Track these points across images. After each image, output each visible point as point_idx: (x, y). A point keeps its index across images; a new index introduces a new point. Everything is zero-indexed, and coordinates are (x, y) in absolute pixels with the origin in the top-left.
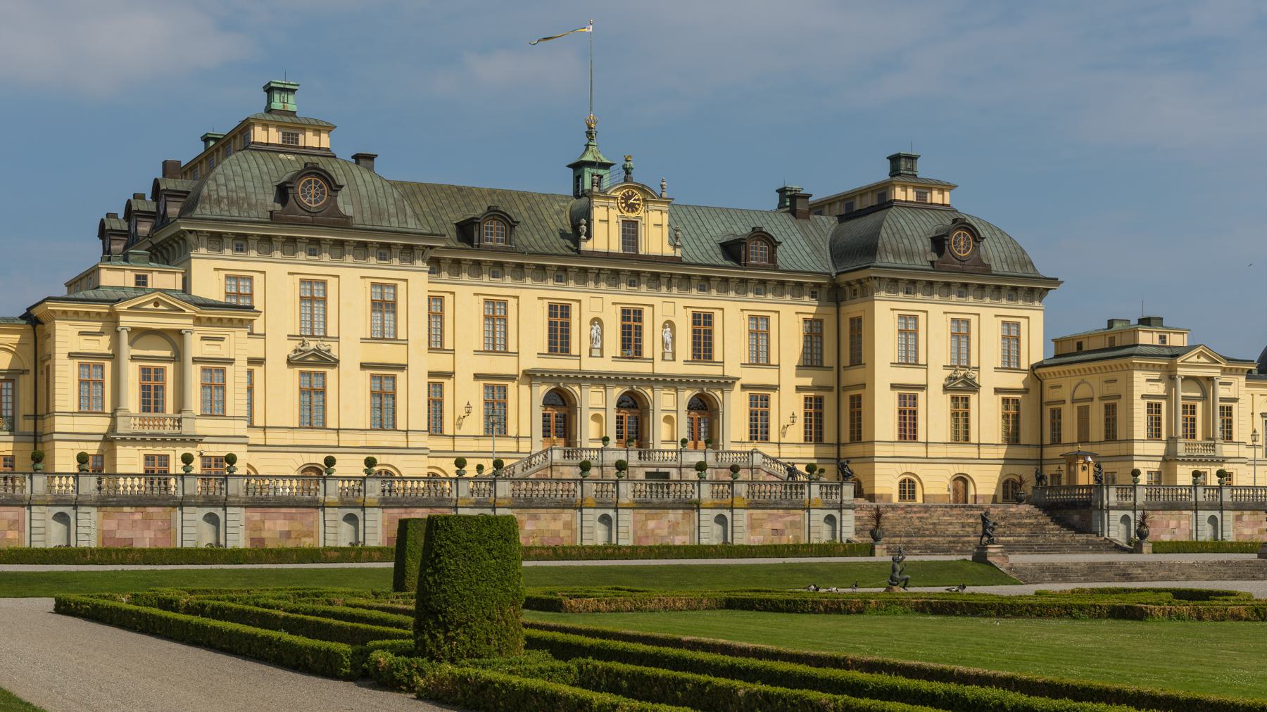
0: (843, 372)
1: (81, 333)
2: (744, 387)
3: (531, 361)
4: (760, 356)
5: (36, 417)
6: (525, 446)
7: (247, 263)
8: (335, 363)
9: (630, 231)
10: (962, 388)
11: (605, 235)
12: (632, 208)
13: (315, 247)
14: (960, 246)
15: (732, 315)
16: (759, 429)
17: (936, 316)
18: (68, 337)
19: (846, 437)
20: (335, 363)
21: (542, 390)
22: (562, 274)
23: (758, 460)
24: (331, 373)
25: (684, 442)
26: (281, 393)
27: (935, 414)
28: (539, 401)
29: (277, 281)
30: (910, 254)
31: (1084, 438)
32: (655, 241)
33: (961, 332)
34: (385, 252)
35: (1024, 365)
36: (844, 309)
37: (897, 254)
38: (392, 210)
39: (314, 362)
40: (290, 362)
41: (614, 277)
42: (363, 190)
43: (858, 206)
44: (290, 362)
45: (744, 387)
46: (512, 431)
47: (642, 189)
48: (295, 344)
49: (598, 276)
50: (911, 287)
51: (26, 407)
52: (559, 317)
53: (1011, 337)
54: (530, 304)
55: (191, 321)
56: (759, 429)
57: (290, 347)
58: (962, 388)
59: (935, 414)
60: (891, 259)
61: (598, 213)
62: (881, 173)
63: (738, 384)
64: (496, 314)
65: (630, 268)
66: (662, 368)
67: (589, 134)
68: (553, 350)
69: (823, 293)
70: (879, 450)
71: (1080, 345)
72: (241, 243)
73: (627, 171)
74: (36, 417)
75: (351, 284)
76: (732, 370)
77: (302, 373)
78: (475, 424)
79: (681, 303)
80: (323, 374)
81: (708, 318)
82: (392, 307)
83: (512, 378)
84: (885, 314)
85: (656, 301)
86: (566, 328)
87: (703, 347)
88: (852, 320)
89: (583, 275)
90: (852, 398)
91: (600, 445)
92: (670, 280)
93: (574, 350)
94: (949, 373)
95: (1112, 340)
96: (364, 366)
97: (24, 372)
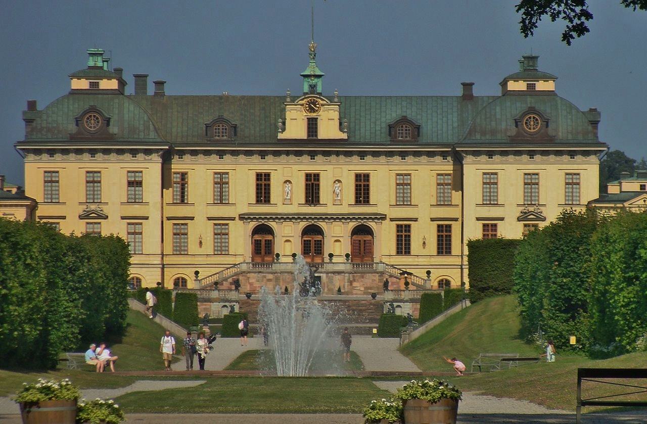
2: (392, 220)
3: (245, 210)
6: (239, 260)
7: (56, 163)
8: (106, 217)
9: (312, 125)
11: (295, 127)
12: (312, 110)
15: (383, 175)
16: (403, 245)
17: (511, 173)
20: (106, 217)
21: (253, 225)
22: (263, 154)
23: (381, 268)
25: (347, 255)
30: (494, 132)
32: (329, 129)
33: (531, 182)
35: (584, 201)
37: (483, 133)
38: (142, 128)
41: (298, 154)
42: (126, 116)
45: (392, 220)
53: (573, 182)
54: (242, 174)
56: (403, 245)
57: (81, 209)
60: (478, 137)
61: (289, 115)
63: (388, 219)
64: (221, 182)
65: (312, 145)
66: (331, 209)
68: (258, 201)
75: (114, 171)
78: (209, 248)
79: (345, 168)
81: (367, 177)
82: (139, 184)
83: (233, 219)
85: (329, 168)
86: (268, 187)
89: (276, 154)
91: (290, 259)
92: (338, 154)
93: (272, 201)
94: (521, 208)
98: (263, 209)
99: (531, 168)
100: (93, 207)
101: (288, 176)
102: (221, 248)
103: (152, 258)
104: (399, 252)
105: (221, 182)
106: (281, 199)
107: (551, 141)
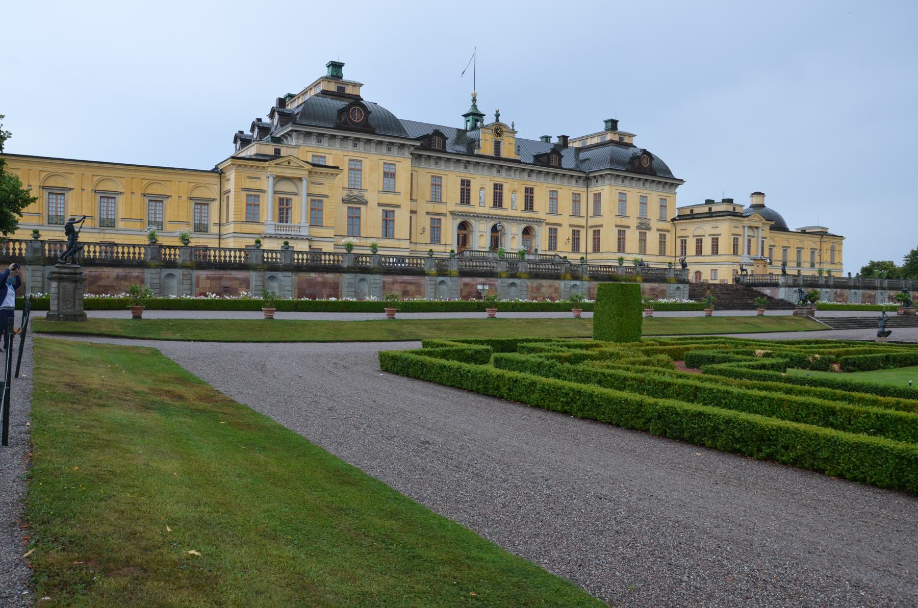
0: (589, 220)
1: (249, 177)
2: (547, 224)
4: (554, 211)
5: (220, 225)
8: (366, 203)
9: (497, 145)
10: (644, 227)
11: (486, 148)
12: (499, 135)
14: (645, 163)
15: (542, 189)
19: (590, 249)
20: (366, 203)
21: (459, 221)
23: (557, 259)
24: (363, 208)
28: (456, 228)
31: (699, 251)
32: (508, 151)
33: (643, 202)
36: (590, 189)
39: (354, 202)
43: (589, 142)
45: (547, 224)
46: (443, 242)
47: (505, 126)
48: (346, 192)
49: (484, 165)
51: (214, 218)
52: (465, 187)
54: (452, 178)
55: (307, 173)
58: (644, 227)
62: (602, 128)
64: (437, 183)
65: (497, 162)
67: (474, 100)
68: (462, 202)
69: (581, 182)
71: (692, 211)
73: (497, 116)
74: (220, 225)
76: (541, 215)
77: (349, 208)
78: (427, 238)
80: (359, 208)
82: (393, 175)
83: (445, 215)
87: (529, 204)
88: (595, 194)
90: (594, 231)
95: (710, 209)
96: (380, 205)
97: (213, 200)
98: (464, 208)
99: (644, 192)
100: (355, 193)
101: (482, 183)
102: (436, 238)
103: (402, 242)
104: (550, 249)
105: (437, 183)
106: (478, 202)
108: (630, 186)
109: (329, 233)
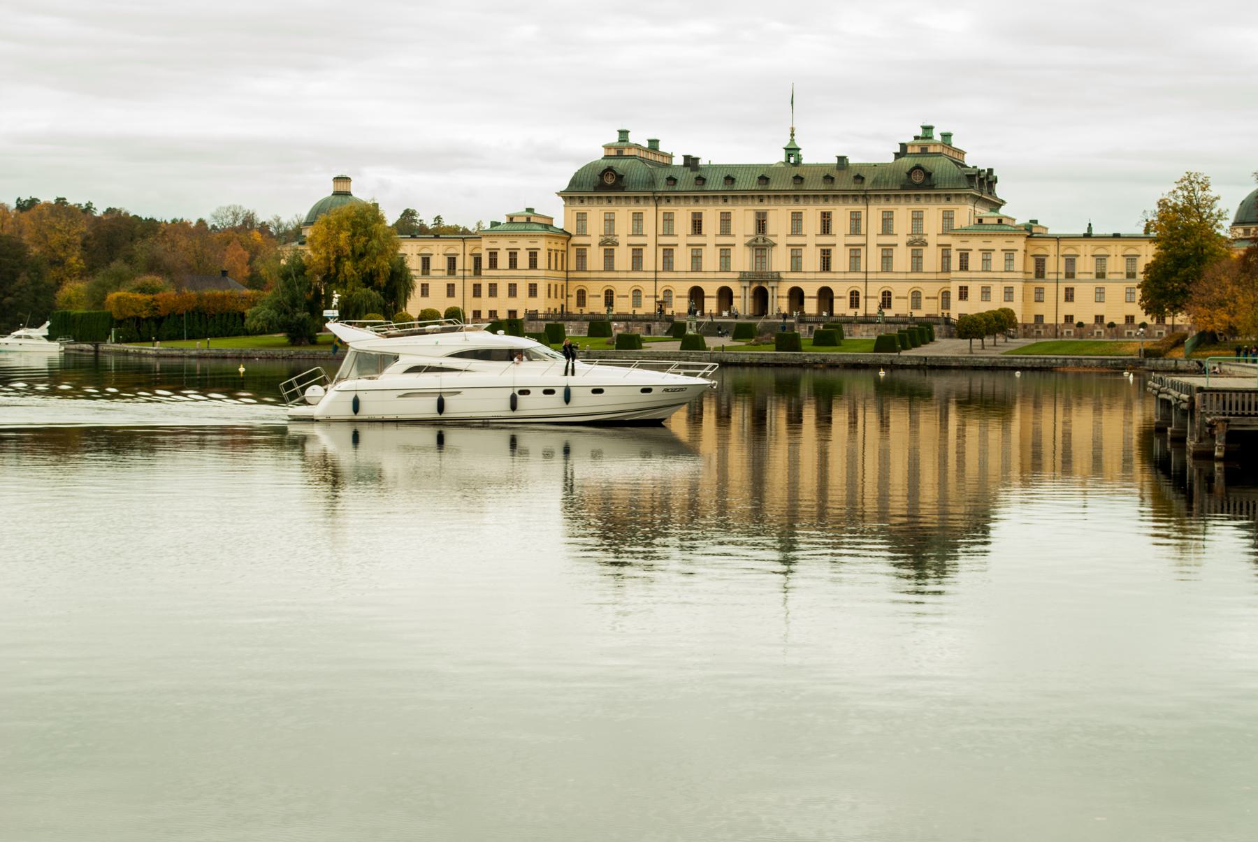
8: (618, 244)
10: (917, 244)
13: (609, 200)
17: (902, 213)
18: (486, 244)
20: (618, 244)
26: (595, 258)
27: (902, 259)
29: (596, 214)
33: (917, 218)
34: (637, 199)
39: (609, 245)
40: (600, 245)
44: (600, 245)
50: (888, 198)
53: (948, 217)
58: (917, 244)
59: (902, 259)
70: (869, 276)
72: (582, 200)
75: (623, 214)
84: (874, 213)
107: (932, 187)
108: (899, 203)
109: (542, 273)
